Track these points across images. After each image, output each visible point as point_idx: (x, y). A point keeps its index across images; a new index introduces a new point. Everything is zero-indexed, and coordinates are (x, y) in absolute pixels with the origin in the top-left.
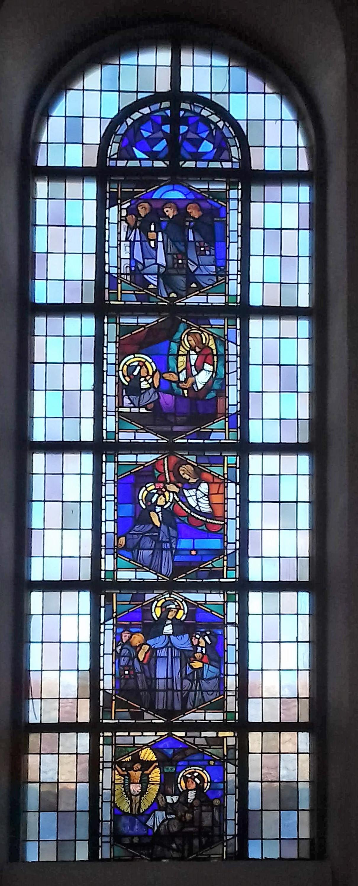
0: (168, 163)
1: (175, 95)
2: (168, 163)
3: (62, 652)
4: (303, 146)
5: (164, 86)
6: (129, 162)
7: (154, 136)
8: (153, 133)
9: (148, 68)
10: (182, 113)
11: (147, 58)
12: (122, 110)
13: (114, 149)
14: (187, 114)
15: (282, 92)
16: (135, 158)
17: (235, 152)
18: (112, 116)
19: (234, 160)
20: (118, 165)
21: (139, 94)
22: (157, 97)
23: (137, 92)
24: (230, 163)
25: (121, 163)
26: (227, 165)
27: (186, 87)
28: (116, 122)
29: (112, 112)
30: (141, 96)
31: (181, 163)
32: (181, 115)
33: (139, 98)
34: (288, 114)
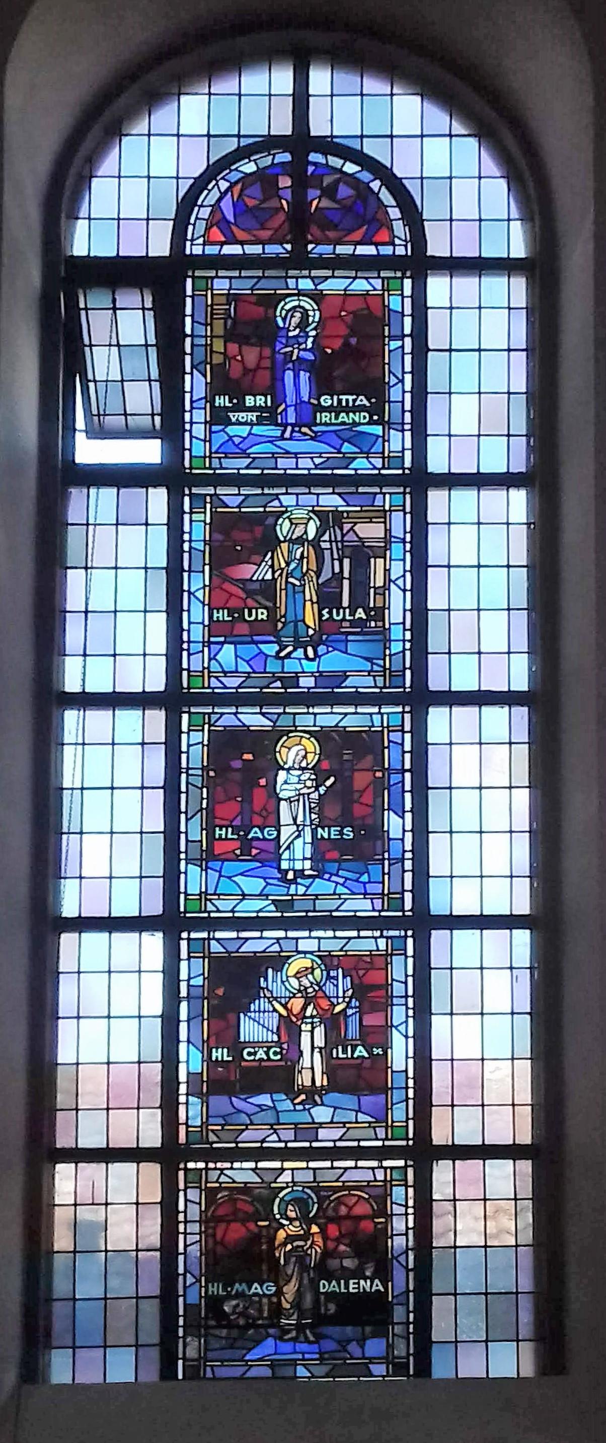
0: (288, 247)
1: (301, 140)
2: (288, 247)
3: (112, 1012)
4: (517, 217)
5: (283, 126)
6: (225, 247)
7: (262, 206)
8: (263, 201)
9: (256, 99)
10: (311, 169)
11: (254, 81)
12: (214, 164)
13: (197, 229)
14: (320, 171)
15: (484, 132)
16: (232, 240)
17: (399, 229)
18: (196, 175)
19: (397, 241)
20: (206, 252)
21: (242, 139)
22: (269, 143)
23: (239, 136)
24: (391, 248)
25: (212, 250)
26: (387, 250)
27: (318, 127)
28: (200, 184)
29: (197, 168)
30: (244, 142)
31: (310, 247)
32: (309, 173)
33: (241, 145)
34: (490, 166)
